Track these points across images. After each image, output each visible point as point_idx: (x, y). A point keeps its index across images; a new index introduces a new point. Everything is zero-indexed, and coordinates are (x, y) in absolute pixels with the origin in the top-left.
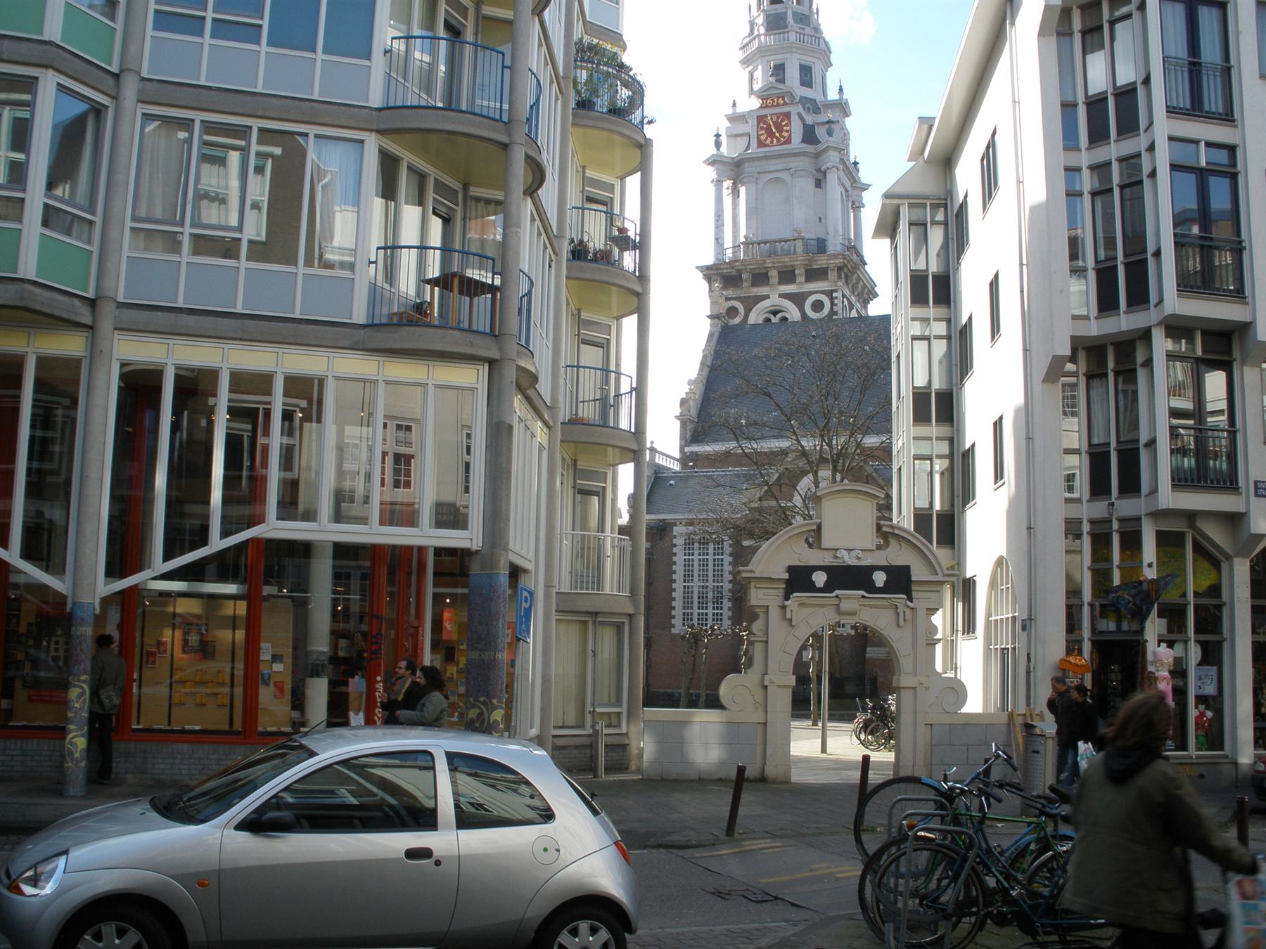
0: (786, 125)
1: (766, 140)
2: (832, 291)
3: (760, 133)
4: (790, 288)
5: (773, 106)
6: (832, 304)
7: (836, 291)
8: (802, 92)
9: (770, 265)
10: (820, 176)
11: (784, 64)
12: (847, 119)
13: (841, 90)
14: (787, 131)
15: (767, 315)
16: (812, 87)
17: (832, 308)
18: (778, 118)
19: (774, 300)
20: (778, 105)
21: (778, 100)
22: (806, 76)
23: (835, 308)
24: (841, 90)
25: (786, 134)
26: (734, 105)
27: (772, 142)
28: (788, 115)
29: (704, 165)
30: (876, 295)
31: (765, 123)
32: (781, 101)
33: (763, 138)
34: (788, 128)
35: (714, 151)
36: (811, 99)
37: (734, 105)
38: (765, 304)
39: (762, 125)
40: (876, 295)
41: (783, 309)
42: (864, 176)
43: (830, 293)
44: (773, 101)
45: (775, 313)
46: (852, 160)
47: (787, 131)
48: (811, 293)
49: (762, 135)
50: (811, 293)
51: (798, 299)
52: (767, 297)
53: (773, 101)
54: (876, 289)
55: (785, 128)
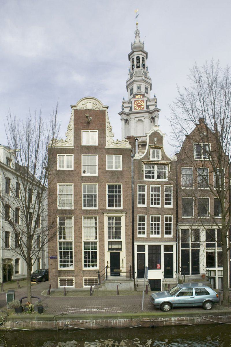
1: (137, 108)
5: (139, 98)
8: (146, 95)
10: (152, 120)
11: (141, 86)
13: (155, 96)
18: (140, 102)
24: (155, 96)
25: (142, 106)
26: (124, 99)
27: (138, 108)
29: (118, 115)
31: (136, 103)
32: (141, 97)
33: (136, 107)
35: (121, 110)
37: (124, 99)
39: (135, 103)
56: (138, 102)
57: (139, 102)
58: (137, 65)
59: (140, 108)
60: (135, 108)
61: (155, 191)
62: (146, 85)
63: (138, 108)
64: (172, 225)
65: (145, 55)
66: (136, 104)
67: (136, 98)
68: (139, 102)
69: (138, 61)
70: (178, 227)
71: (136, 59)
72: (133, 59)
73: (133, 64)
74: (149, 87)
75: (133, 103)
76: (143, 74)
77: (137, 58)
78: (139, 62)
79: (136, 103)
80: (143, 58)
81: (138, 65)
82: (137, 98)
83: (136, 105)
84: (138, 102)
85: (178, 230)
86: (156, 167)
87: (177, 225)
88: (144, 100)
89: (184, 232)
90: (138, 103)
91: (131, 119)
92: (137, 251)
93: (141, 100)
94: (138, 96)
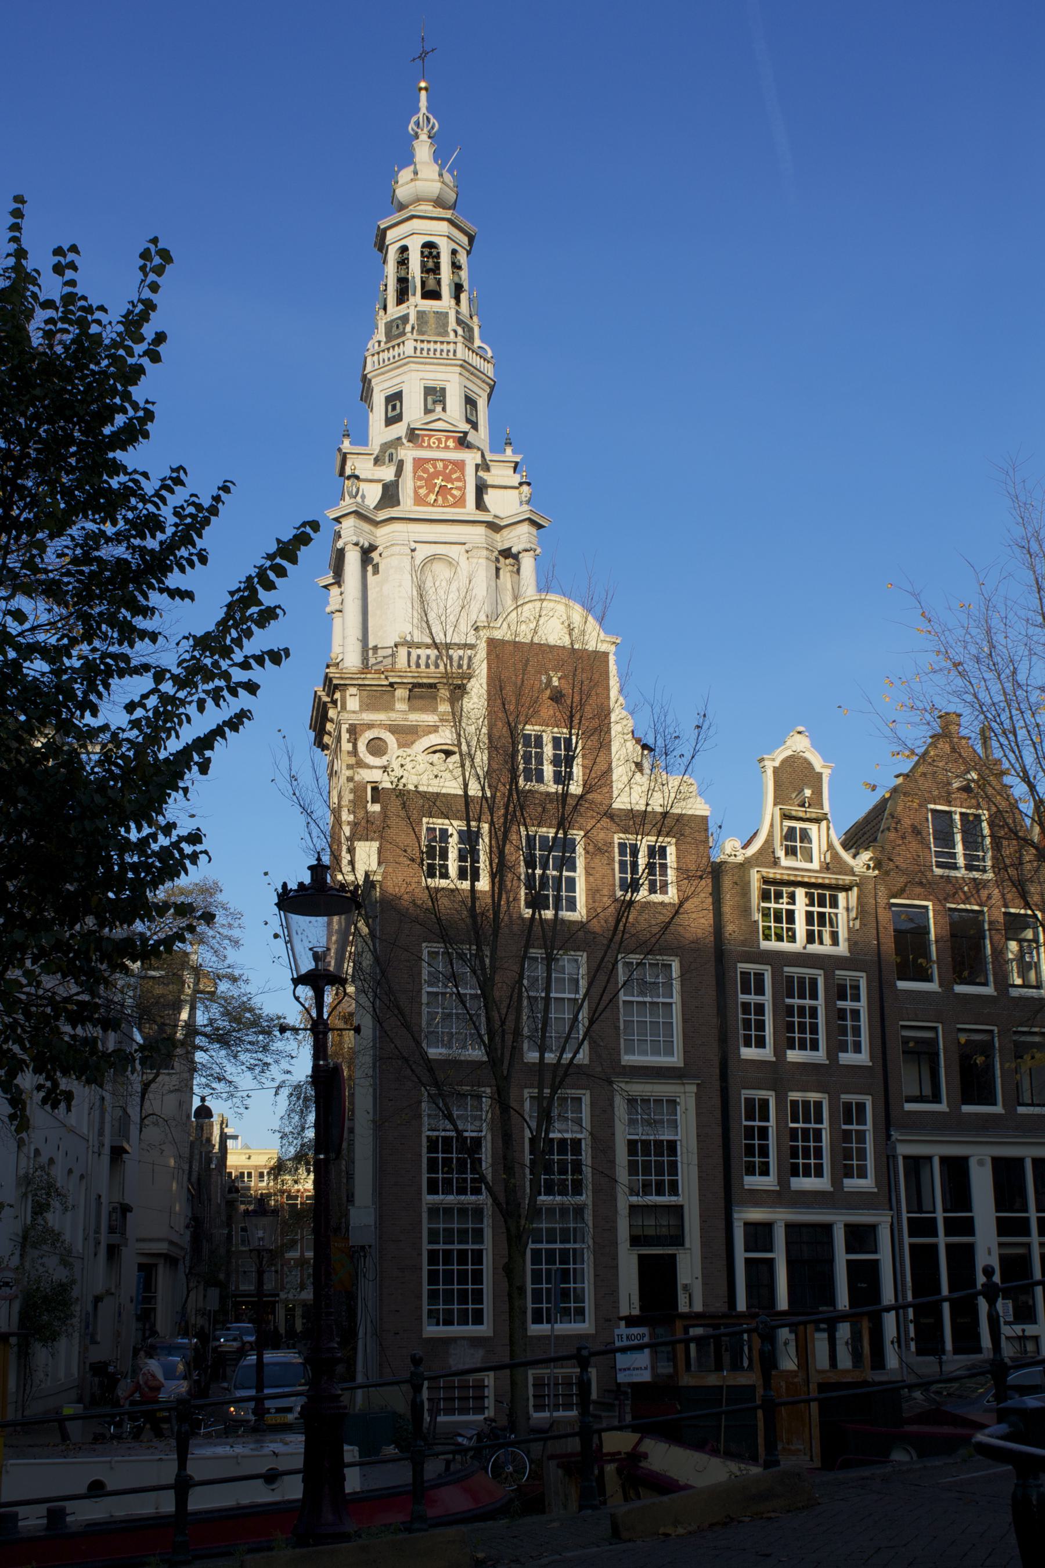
0: (458, 479)
1: (427, 495)
3: (419, 483)
14: (457, 488)
18: (445, 467)
20: (447, 447)
21: (448, 438)
25: (454, 492)
28: (460, 465)
31: (426, 471)
32: (451, 443)
33: (423, 492)
34: (459, 484)
44: (439, 440)
47: (457, 488)
49: (421, 487)
52: (434, 729)
53: (439, 440)
56: (435, 467)
57: (440, 465)
58: (423, 283)
59: (445, 499)
60: (416, 492)
61: (802, 996)
62: (470, 385)
64: (869, 1138)
65: (465, 240)
66: (425, 476)
67: (426, 444)
68: (440, 465)
69: (431, 265)
70: (895, 1148)
71: (422, 253)
72: (404, 249)
73: (403, 274)
74: (485, 396)
75: (408, 467)
76: (460, 331)
77: (426, 251)
78: (436, 269)
79: (426, 471)
80: (454, 252)
81: (431, 284)
82: (429, 446)
83: (423, 483)
84: (435, 467)
85: (895, 1157)
86: (800, 893)
87: (889, 1137)
88: (463, 462)
89: (916, 1164)
90: (432, 470)
92: (746, 1250)
93: (450, 461)
94: (432, 440)
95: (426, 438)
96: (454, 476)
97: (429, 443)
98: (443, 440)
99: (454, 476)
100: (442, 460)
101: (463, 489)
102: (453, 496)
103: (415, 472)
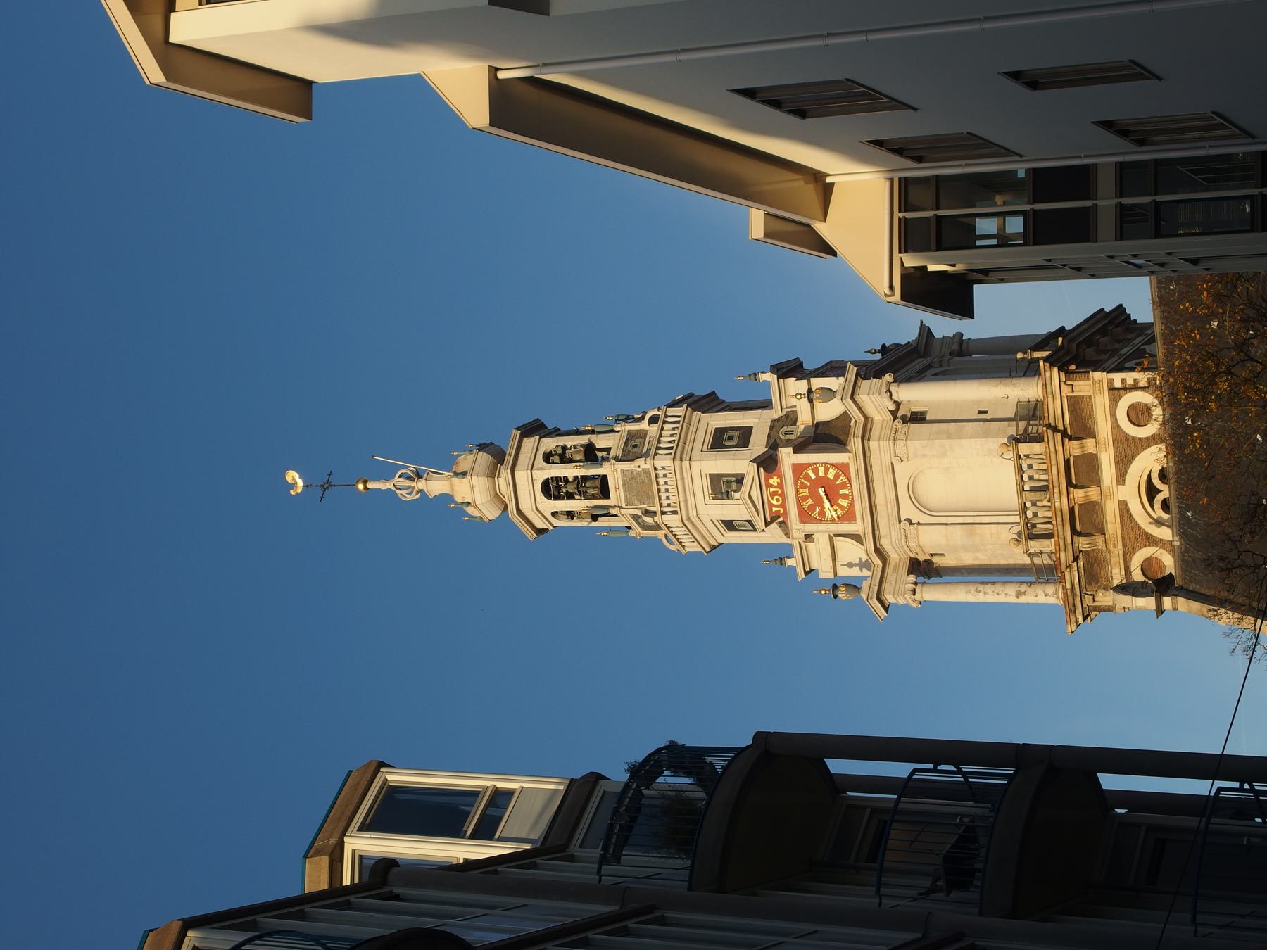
0: (816, 471)
2: (1112, 389)
4: (1107, 463)
5: (782, 495)
6: (1135, 387)
7: (1111, 382)
9: (1065, 500)
12: (806, 366)
14: (826, 471)
15: (1157, 505)
16: (752, 427)
17: (1143, 389)
18: (803, 486)
19: (1131, 492)
20: (780, 486)
21: (771, 486)
22: (731, 438)
23: (1143, 383)
25: (831, 475)
27: (845, 497)
28: (798, 469)
30: (1120, 309)
31: (812, 508)
34: (821, 469)
36: (772, 428)
38: (1136, 508)
39: (816, 514)
40: (1120, 309)
41: (1145, 477)
42: (908, 335)
43: (1116, 393)
44: (773, 494)
45: (1152, 492)
46: (878, 356)
47: (826, 471)
48: (1116, 426)
50: (1116, 426)
51: (1127, 451)
53: (773, 494)
54: (1107, 310)
55: (821, 474)
56: (805, 498)
59: (843, 486)
63: (842, 502)
72: (554, 514)
80: (547, 458)
84: (805, 498)
91: (912, 544)
94: (774, 502)
95: (774, 509)
96: (813, 477)
97: (776, 506)
98: (772, 490)
99: (813, 477)
100: (797, 491)
101: (827, 467)
102: (837, 477)
103: (819, 521)
